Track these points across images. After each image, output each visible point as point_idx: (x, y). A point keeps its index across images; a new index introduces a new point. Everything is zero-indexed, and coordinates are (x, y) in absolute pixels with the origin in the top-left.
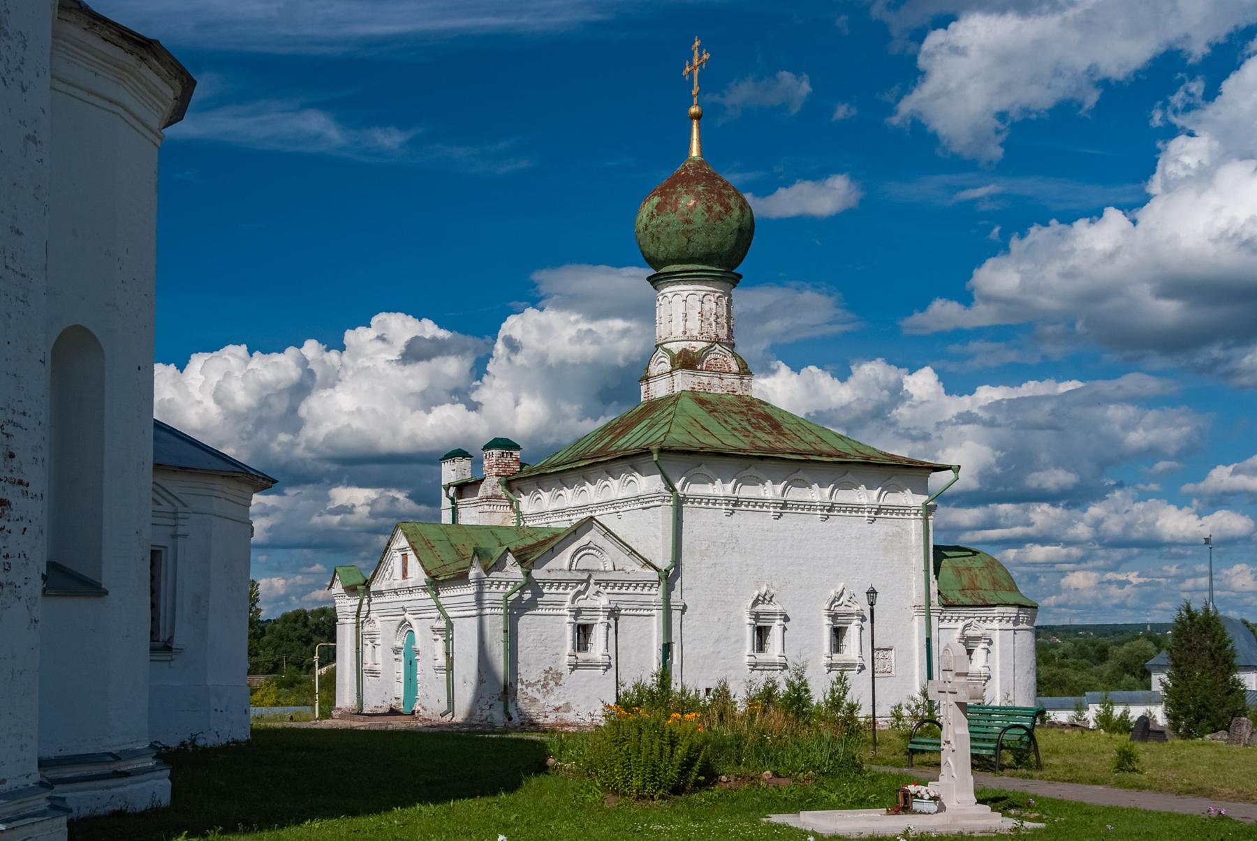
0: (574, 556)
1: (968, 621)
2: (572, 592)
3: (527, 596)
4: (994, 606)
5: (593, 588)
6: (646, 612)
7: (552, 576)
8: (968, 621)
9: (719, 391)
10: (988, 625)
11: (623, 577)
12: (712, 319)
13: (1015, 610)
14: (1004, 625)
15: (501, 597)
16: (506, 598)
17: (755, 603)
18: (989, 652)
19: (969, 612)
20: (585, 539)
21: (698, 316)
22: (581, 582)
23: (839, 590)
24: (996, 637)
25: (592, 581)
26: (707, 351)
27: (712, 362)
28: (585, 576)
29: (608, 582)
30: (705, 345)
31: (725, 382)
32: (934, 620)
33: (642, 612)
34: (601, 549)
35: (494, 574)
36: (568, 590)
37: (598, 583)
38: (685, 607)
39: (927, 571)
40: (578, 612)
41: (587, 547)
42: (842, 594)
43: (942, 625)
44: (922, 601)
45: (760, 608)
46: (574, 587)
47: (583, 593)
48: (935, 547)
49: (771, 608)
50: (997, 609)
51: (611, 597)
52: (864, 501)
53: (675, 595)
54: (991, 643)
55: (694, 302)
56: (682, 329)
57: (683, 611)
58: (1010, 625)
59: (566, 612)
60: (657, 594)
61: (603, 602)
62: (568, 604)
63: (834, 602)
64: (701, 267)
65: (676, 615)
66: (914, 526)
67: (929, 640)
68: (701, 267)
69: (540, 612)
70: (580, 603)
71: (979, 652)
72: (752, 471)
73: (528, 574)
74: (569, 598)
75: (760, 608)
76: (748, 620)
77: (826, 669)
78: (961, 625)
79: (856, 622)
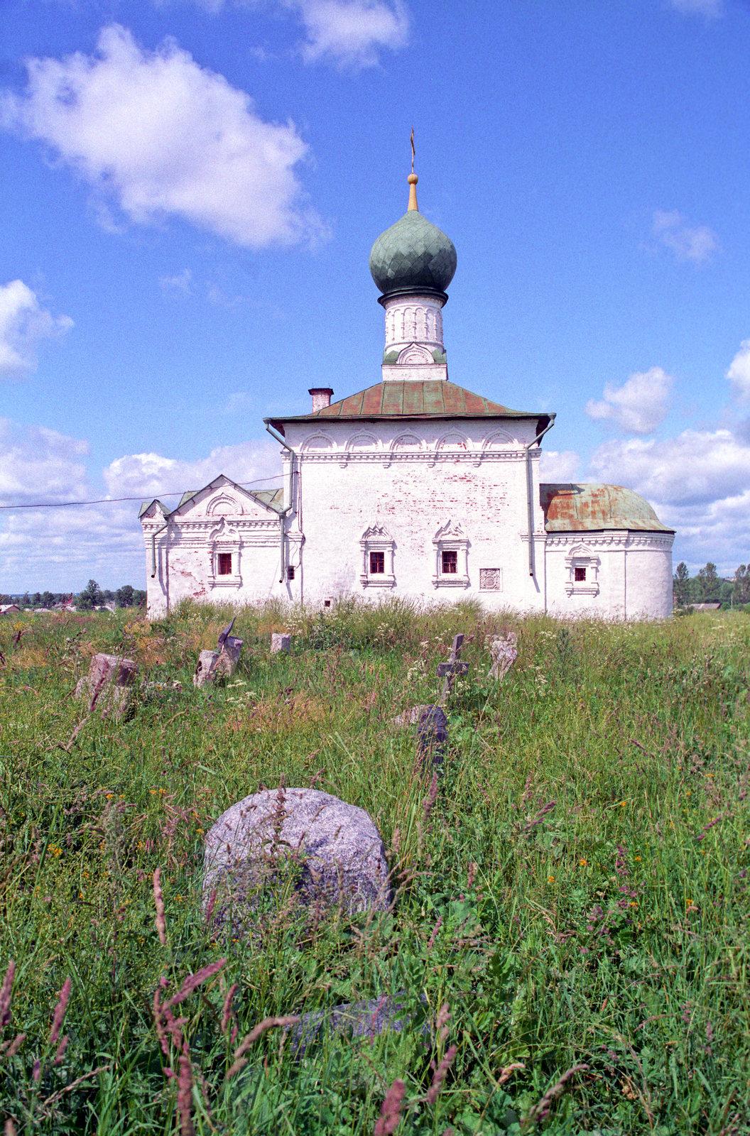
1: (575, 545)
2: (211, 531)
5: (227, 528)
6: (273, 544)
8: (575, 545)
10: (598, 547)
11: (249, 518)
13: (626, 533)
15: (150, 536)
17: (366, 534)
18: (597, 571)
19: (578, 537)
20: (217, 493)
22: (216, 523)
24: (604, 558)
26: (406, 351)
28: (218, 519)
29: (238, 523)
30: (407, 345)
32: (539, 546)
33: (267, 544)
36: (207, 530)
37: (230, 523)
38: (304, 538)
39: (530, 504)
42: (449, 524)
43: (548, 548)
44: (526, 531)
49: (382, 538)
51: (242, 533)
54: (599, 562)
55: (409, 317)
59: (207, 546)
60: (276, 531)
71: (589, 573)
75: (370, 539)
76: (359, 547)
77: (434, 587)
78: (568, 547)
79: (461, 548)
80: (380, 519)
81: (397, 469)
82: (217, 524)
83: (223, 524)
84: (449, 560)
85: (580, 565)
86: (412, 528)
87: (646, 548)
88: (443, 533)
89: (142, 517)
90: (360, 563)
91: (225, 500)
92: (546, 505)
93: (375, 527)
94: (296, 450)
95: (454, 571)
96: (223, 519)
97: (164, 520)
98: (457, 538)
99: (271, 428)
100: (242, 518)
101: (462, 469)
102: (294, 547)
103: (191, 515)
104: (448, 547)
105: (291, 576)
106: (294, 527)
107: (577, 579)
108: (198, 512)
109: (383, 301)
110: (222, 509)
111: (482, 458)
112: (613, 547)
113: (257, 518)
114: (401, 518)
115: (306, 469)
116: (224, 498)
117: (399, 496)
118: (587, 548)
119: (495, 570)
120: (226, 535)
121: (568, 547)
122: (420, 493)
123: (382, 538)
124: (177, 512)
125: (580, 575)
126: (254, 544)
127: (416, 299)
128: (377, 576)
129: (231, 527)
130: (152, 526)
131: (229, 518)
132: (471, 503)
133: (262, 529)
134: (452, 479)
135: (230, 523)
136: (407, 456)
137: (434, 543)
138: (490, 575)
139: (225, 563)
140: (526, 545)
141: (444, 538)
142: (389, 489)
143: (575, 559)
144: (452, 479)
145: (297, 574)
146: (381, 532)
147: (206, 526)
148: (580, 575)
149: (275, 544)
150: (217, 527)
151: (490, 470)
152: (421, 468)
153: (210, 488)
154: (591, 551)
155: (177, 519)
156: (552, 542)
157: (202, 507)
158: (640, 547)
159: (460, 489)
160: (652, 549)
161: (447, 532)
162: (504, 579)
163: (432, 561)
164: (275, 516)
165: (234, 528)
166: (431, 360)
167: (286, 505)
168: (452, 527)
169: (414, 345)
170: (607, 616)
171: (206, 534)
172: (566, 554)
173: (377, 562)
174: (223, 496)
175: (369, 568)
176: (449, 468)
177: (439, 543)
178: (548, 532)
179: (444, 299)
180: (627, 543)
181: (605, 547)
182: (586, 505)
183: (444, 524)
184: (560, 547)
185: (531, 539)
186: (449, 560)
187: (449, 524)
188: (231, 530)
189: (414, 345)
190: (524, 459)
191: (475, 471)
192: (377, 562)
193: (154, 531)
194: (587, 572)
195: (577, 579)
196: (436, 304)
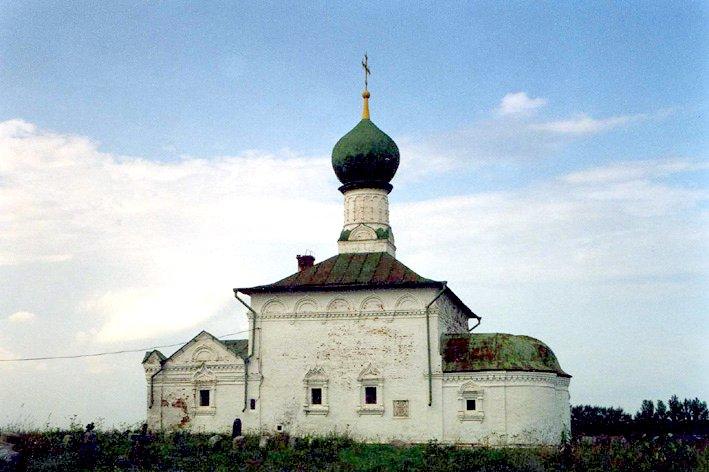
1: (466, 382)
11: (222, 363)
24: (486, 390)
32: (438, 383)
37: (209, 367)
40: (197, 383)
45: (314, 377)
49: (320, 377)
67: (431, 397)
71: (478, 404)
76: (303, 385)
80: (321, 362)
81: (330, 326)
84: (371, 395)
86: (342, 370)
89: (144, 362)
90: (305, 396)
94: (258, 311)
98: (374, 377)
99: (239, 294)
100: (218, 363)
101: (380, 324)
102: (254, 385)
103: (178, 362)
104: (371, 384)
105: (253, 407)
106: (254, 368)
110: (204, 356)
112: (495, 384)
113: (228, 363)
114: (334, 362)
115: (264, 325)
117: (334, 345)
120: (206, 376)
121: (460, 384)
122: (348, 342)
123: (320, 377)
125: (471, 405)
128: (317, 407)
131: (207, 363)
132: (387, 350)
134: (374, 331)
135: (209, 367)
136: (338, 315)
138: (401, 408)
140: (428, 381)
141: (368, 377)
142: (326, 340)
144: (374, 331)
145: (257, 405)
148: (471, 405)
150: (199, 370)
151: (401, 325)
152: (350, 325)
153: (195, 340)
154: (479, 386)
157: (188, 355)
159: (378, 340)
162: (412, 408)
163: (360, 395)
166: (375, 236)
167: (250, 353)
170: (493, 442)
171: (192, 375)
173: (317, 396)
175: (310, 400)
176: (370, 323)
179: (389, 188)
182: (477, 350)
183: (366, 366)
184: (453, 384)
185: (430, 376)
186: (371, 395)
191: (390, 325)
192: (317, 396)
193: (153, 373)
194: (476, 403)
196: (382, 193)
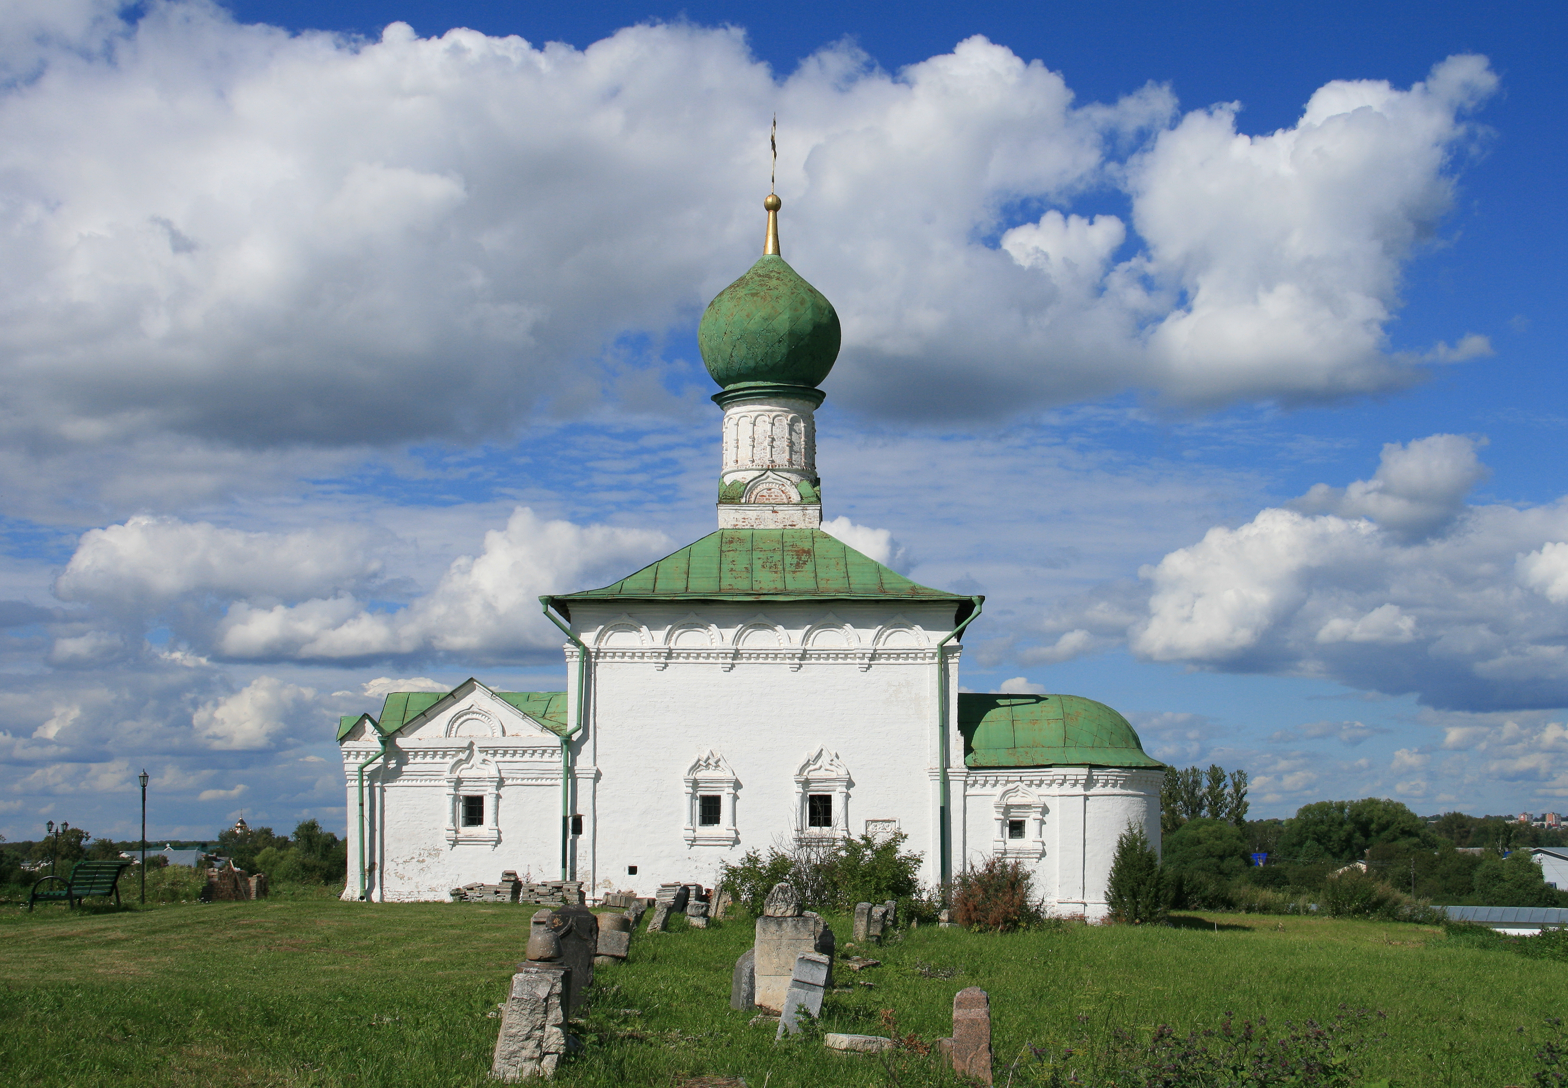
0: (452, 721)
1: (1010, 786)
2: (450, 761)
3: (392, 764)
4: (1050, 766)
5: (478, 757)
6: (549, 782)
7: (424, 744)
8: (1010, 786)
9: (772, 526)
10: (1044, 789)
12: (766, 443)
13: (1085, 771)
14: (1067, 789)
15: (356, 768)
16: (361, 770)
19: (1014, 774)
21: (749, 441)
22: (462, 749)
23: (815, 753)
24: (1054, 805)
25: (475, 748)
27: (765, 493)
30: (757, 473)
31: (780, 515)
32: (956, 788)
33: (544, 782)
34: (485, 714)
35: (348, 744)
36: (447, 759)
41: (468, 711)
42: (820, 755)
46: (453, 756)
47: (468, 760)
48: (962, 697)
50: (1054, 771)
51: (501, 766)
52: (855, 644)
53: (584, 762)
55: (763, 426)
56: (734, 458)
57: (598, 776)
58: (1079, 790)
59: (445, 783)
60: (557, 762)
61: (491, 770)
62: (447, 774)
63: (808, 764)
64: (753, 384)
65: (584, 787)
66: (930, 672)
68: (753, 384)
69: (401, 783)
70: (464, 772)
71: (1031, 827)
72: (760, 618)
73: (388, 740)
74: (447, 767)
75: (699, 775)
78: (1000, 789)
79: (839, 789)
82: (463, 752)
83: (472, 751)
85: (1015, 815)
87: (1117, 790)
88: (812, 767)
90: (685, 809)
91: (474, 716)
92: (967, 727)
93: (708, 758)
94: (588, 638)
95: (828, 822)
96: (472, 744)
97: (380, 745)
107: (1012, 836)
108: (431, 733)
109: (721, 400)
111: (872, 658)
116: (474, 713)
118: (1028, 791)
119: (889, 821)
121: (1000, 789)
124: (399, 731)
126: (519, 782)
127: (773, 400)
129: (483, 756)
130: (358, 754)
133: (534, 759)
135: (484, 750)
137: (798, 782)
139: (473, 810)
141: (813, 775)
143: (1008, 808)
146: (717, 766)
147: (444, 755)
149: (553, 782)
150: (462, 756)
155: (401, 742)
156: (975, 782)
158: (1109, 790)
160: (1130, 792)
161: (817, 766)
164: (556, 741)
165: (489, 757)
166: (796, 498)
168: (824, 760)
169: (769, 473)
172: (996, 799)
174: (474, 709)
177: (806, 783)
178: (970, 768)
180: (1089, 783)
181: (1055, 789)
184: (988, 789)
187: (820, 755)
188: (484, 760)
189: (769, 473)
190: (936, 660)
193: (361, 760)
195: (1012, 836)
